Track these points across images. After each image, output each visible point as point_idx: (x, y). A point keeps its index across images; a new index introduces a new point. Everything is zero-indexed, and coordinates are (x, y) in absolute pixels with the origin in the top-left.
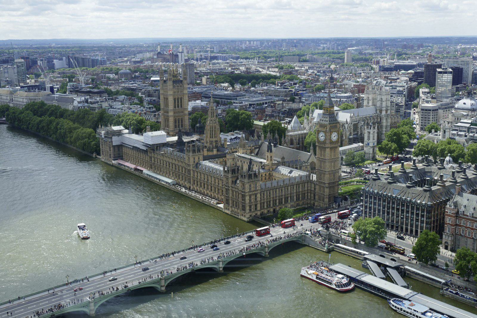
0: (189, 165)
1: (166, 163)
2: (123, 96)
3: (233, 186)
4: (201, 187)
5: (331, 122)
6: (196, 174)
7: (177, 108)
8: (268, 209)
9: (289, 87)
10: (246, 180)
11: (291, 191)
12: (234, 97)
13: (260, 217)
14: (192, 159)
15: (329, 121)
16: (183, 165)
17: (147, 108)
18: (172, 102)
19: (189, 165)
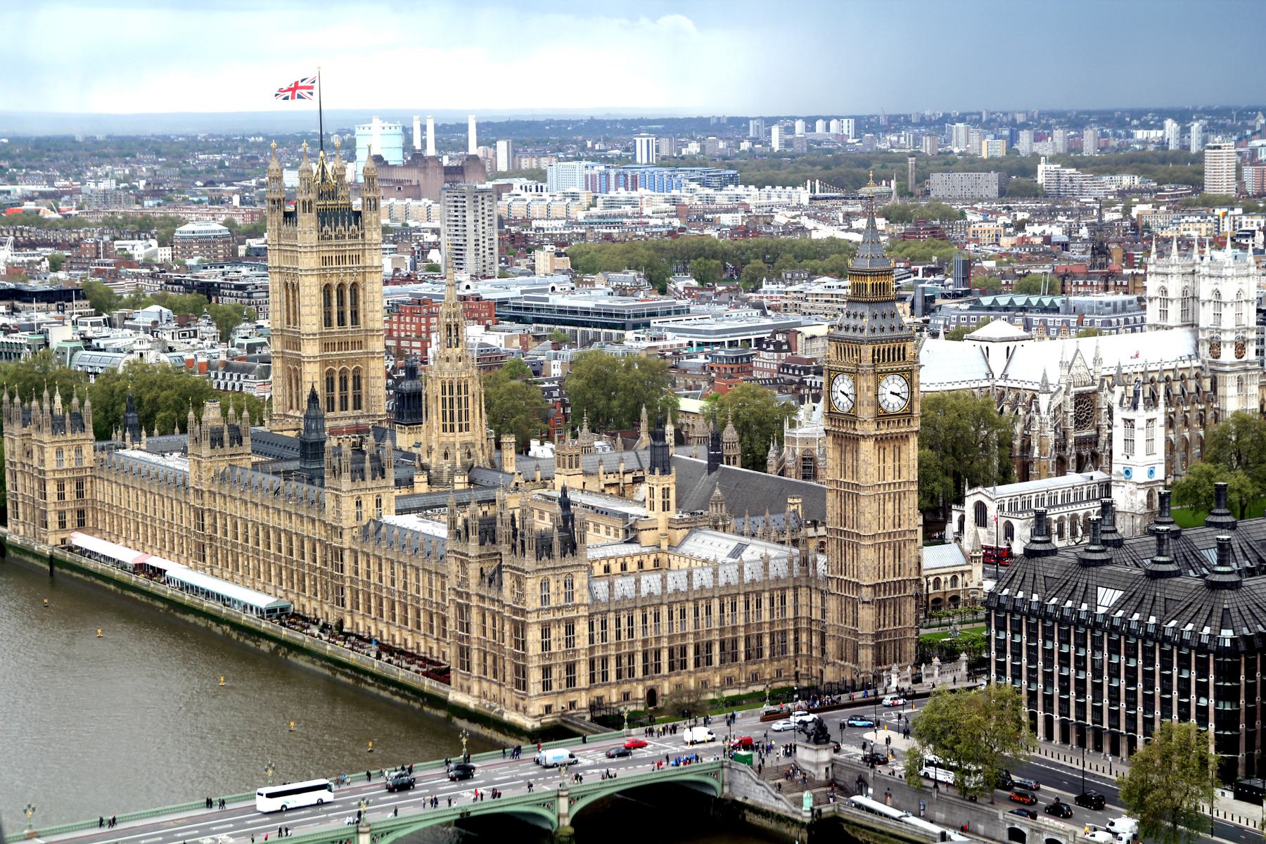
0: (338, 531)
1: (257, 534)
2: (155, 308)
4: (382, 616)
5: (878, 334)
6: (362, 565)
7: (336, 328)
8: (626, 688)
10: (529, 562)
11: (722, 617)
12: (636, 316)
13: (588, 717)
14: (348, 505)
15: (873, 330)
16: (319, 532)
17: (240, 346)
18: (314, 300)
19: (336, 528)
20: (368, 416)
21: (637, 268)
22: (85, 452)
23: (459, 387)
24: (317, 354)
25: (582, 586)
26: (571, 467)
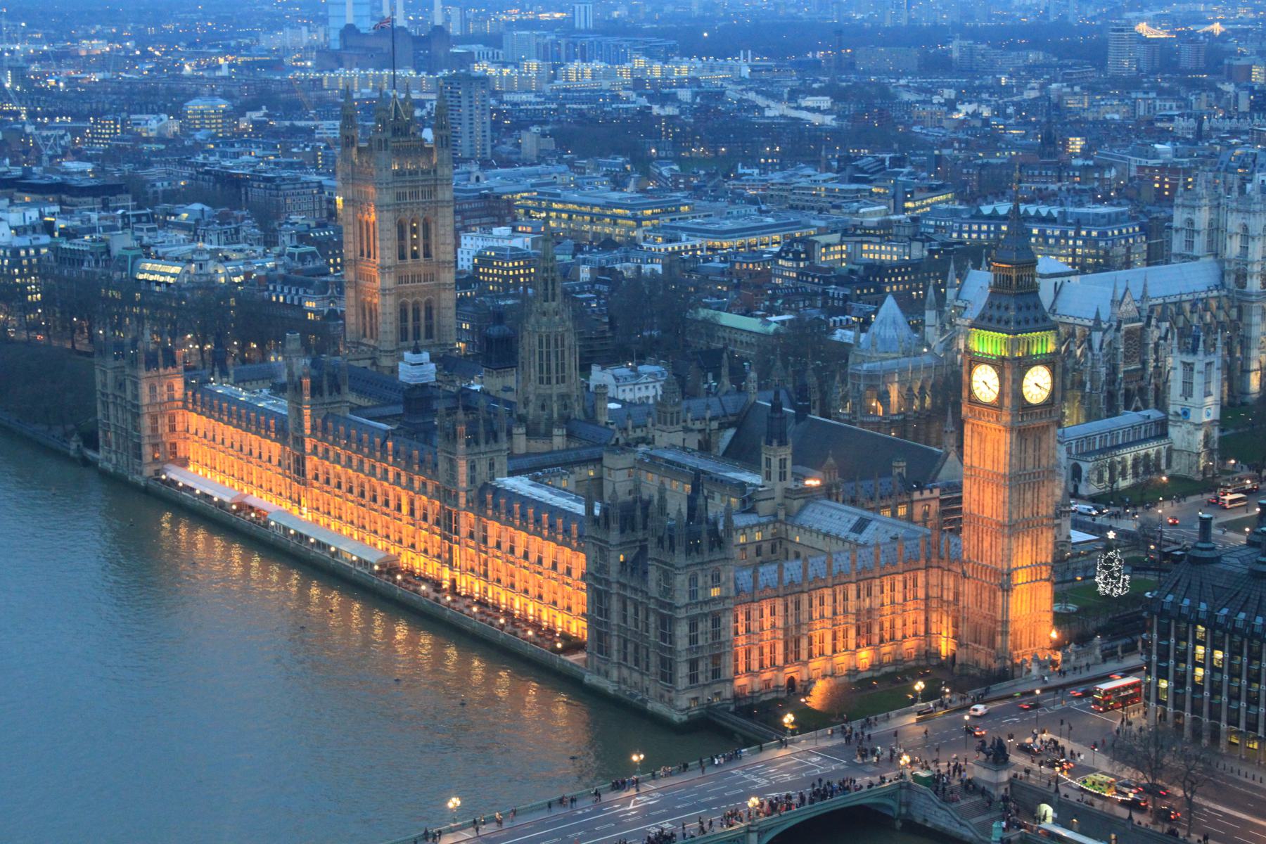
2: (197, 206)
3: (622, 580)
7: (409, 260)
9: (873, 173)
10: (680, 559)
13: (732, 708)
14: (463, 469)
17: (291, 255)
20: (440, 345)
21: (624, 156)
22: (176, 387)
23: (556, 340)
24: (392, 286)
25: (728, 579)
26: (672, 424)
